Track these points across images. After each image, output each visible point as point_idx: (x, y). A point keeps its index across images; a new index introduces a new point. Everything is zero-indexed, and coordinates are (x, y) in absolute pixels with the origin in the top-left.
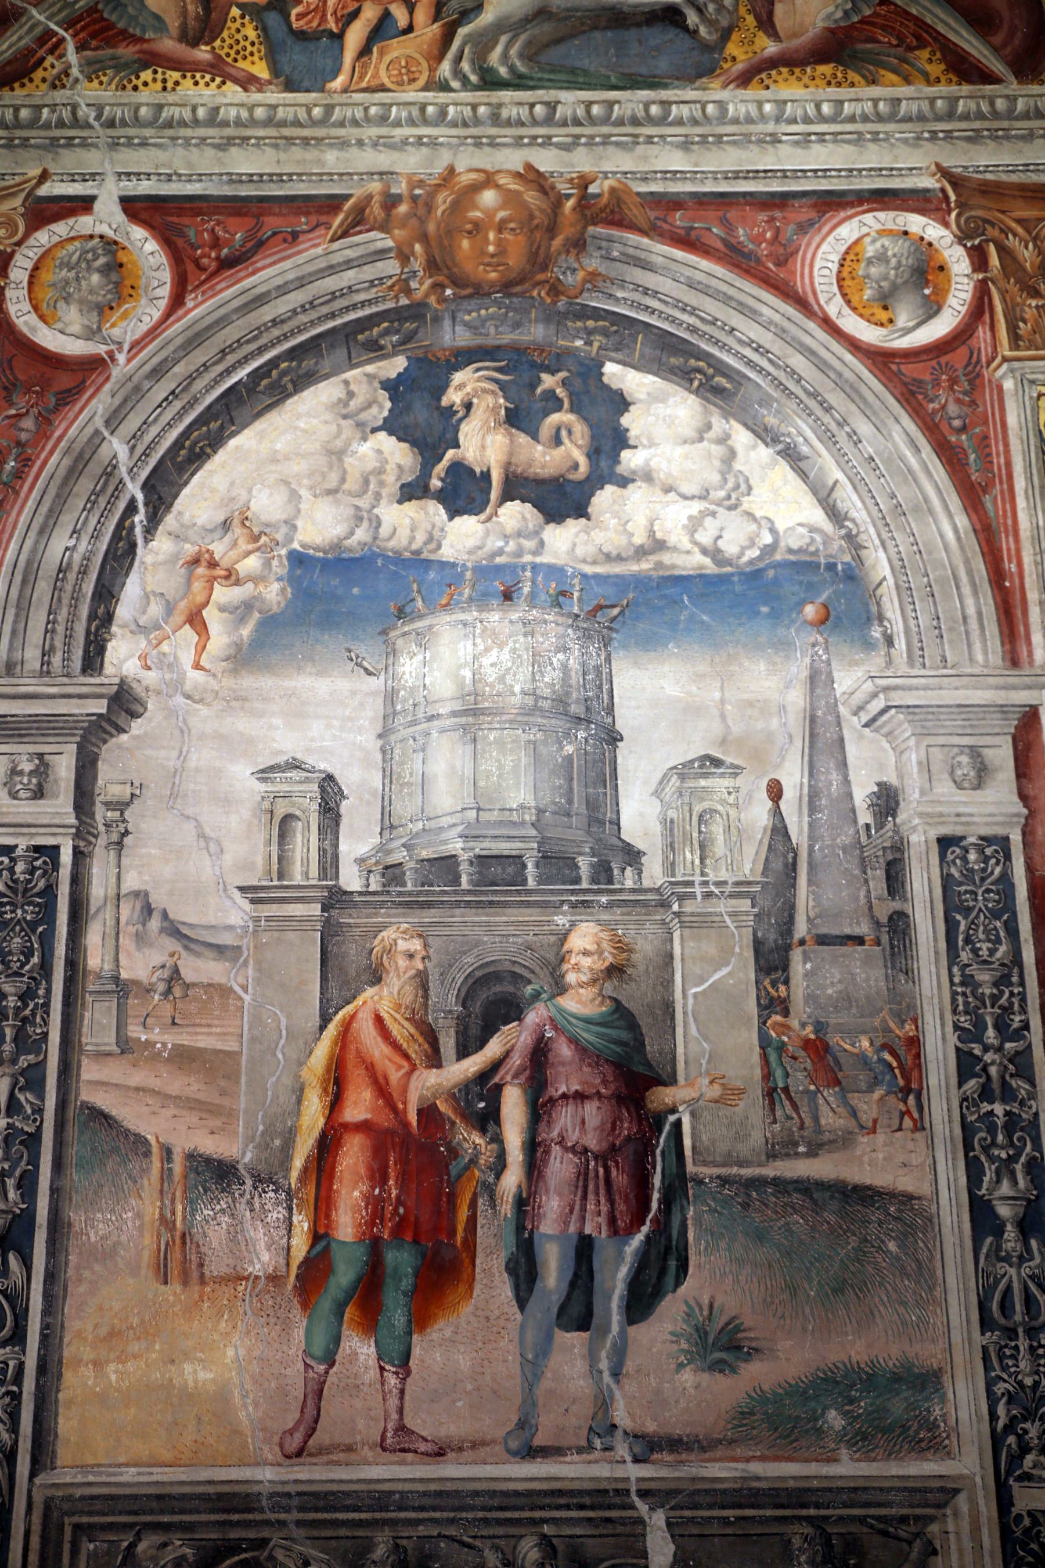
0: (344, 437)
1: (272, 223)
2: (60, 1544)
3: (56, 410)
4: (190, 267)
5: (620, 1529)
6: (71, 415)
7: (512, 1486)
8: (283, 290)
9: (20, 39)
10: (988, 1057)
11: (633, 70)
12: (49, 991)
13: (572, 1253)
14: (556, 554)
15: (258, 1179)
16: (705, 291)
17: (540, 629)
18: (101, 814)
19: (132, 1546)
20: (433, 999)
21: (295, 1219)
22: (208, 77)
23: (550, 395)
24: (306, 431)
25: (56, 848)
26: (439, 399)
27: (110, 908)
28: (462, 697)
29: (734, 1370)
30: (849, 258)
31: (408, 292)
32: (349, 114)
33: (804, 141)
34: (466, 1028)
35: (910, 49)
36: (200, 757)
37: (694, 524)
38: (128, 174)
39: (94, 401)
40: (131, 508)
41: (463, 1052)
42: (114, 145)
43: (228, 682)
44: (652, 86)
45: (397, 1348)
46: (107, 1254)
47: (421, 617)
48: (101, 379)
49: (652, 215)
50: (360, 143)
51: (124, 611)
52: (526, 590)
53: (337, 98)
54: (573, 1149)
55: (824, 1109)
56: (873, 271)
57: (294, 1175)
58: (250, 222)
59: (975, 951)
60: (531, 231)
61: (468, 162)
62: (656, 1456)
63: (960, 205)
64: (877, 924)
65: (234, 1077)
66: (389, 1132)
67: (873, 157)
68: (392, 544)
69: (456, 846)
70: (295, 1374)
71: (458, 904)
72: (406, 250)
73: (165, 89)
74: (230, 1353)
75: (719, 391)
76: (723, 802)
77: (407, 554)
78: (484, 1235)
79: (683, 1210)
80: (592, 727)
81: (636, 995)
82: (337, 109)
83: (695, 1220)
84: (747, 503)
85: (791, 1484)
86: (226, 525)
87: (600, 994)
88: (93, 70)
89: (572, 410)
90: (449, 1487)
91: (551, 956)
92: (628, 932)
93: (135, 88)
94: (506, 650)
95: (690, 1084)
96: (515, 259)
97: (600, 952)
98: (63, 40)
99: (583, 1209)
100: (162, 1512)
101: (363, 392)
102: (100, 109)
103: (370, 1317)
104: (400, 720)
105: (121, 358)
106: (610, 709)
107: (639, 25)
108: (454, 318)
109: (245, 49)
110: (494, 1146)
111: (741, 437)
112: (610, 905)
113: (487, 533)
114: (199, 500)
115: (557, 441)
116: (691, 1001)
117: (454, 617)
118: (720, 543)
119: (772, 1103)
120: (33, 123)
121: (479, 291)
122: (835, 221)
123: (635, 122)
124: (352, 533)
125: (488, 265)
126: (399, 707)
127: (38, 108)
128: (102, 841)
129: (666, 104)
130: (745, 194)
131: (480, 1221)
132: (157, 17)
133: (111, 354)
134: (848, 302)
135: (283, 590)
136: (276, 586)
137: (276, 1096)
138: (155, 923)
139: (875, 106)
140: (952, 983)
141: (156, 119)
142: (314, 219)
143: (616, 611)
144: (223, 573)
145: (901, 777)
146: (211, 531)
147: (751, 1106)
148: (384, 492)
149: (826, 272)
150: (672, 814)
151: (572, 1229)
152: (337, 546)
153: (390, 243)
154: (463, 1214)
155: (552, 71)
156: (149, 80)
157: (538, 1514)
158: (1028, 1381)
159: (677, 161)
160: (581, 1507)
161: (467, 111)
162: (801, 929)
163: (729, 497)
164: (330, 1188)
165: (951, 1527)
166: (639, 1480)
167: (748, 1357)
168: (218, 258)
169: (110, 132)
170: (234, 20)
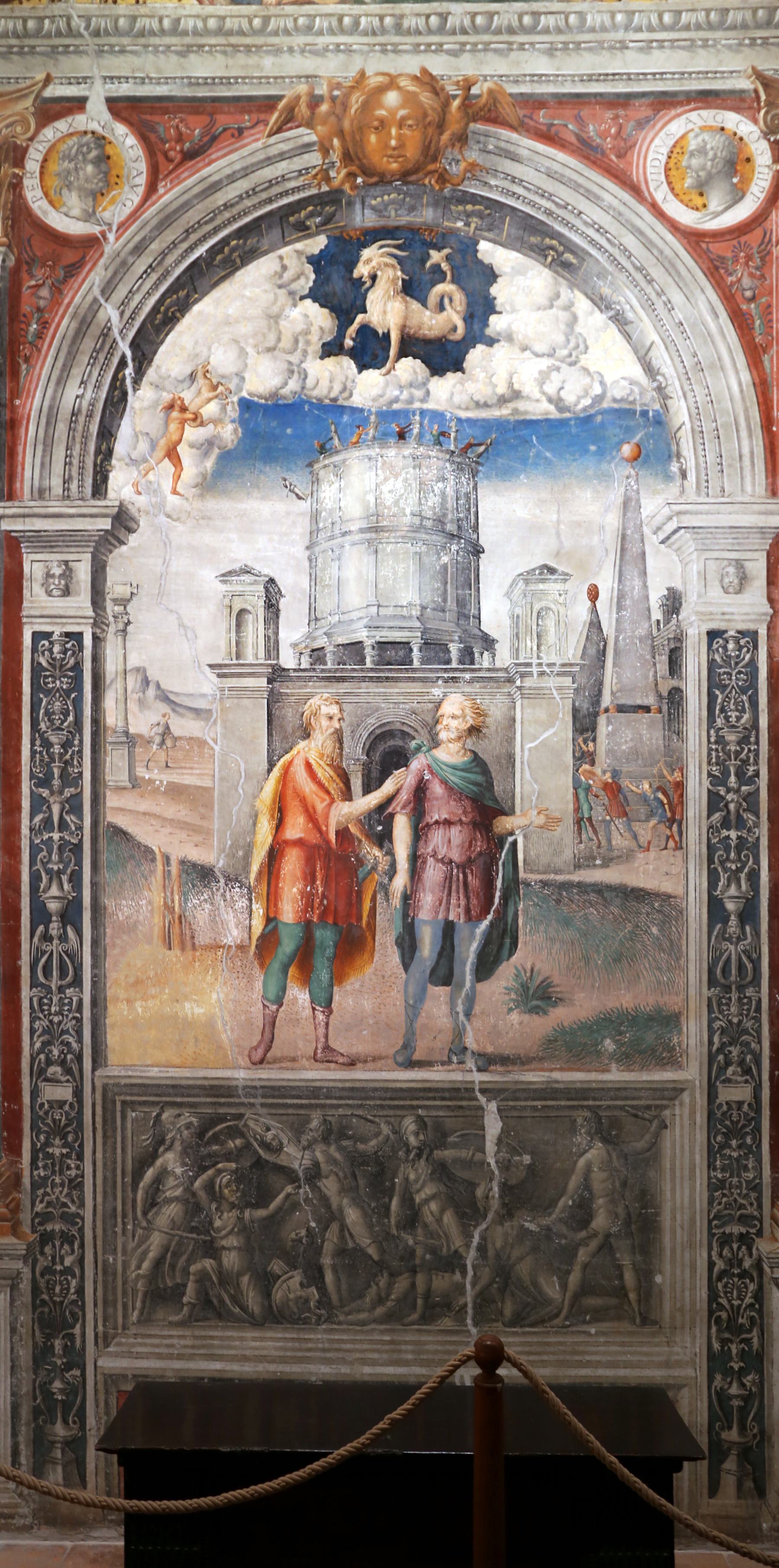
0: (279, 304)
1: (222, 120)
2: (114, 1112)
3: (65, 281)
4: (161, 159)
5: (468, 1113)
6: (76, 285)
7: (398, 1085)
8: (232, 178)
10: (729, 797)
12: (81, 741)
13: (440, 933)
14: (438, 402)
15: (228, 879)
17: (426, 462)
18: (111, 609)
19: (159, 1115)
20: (346, 750)
21: (254, 907)
23: (437, 268)
24: (250, 299)
25: (80, 634)
26: (352, 272)
27: (120, 680)
28: (368, 517)
29: (545, 1013)
31: (328, 179)
32: (282, 24)
34: (369, 771)
36: (179, 563)
37: (543, 378)
38: (112, 78)
39: (92, 274)
40: (123, 364)
41: (367, 789)
42: (100, 52)
43: (197, 504)
45: (323, 996)
46: (130, 928)
47: (337, 452)
48: (97, 255)
50: (291, 50)
51: (121, 447)
52: (416, 431)
54: (442, 861)
55: (615, 834)
57: (253, 876)
58: (206, 119)
59: (727, 718)
61: (376, 66)
62: (492, 1068)
64: (660, 696)
65: (209, 806)
66: (317, 847)
68: (315, 393)
69: (362, 635)
70: (257, 1010)
71: (363, 679)
72: (327, 144)
74: (214, 996)
75: (566, 265)
76: (556, 602)
77: (327, 401)
78: (381, 920)
79: (516, 904)
80: (461, 539)
81: (488, 749)
82: (273, 20)
83: (524, 911)
84: (584, 360)
85: (579, 1085)
86: (192, 377)
87: (464, 748)
89: (453, 281)
90: (358, 1085)
91: (429, 719)
92: (484, 702)
94: (400, 479)
95: (524, 814)
96: (412, 152)
97: (464, 716)
99: (448, 903)
100: (176, 1095)
101: (294, 265)
103: (306, 976)
104: (322, 535)
105: (111, 237)
106: (476, 528)
108: (363, 203)
110: (388, 858)
111: (582, 304)
112: (472, 681)
113: (387, 384)
114: (173, 355)
115: (441, 308)
116: (526, 753)
117: (362, 453)
118: (562, 393)
119: (580, 829)
121: (382, 180)
124: (286, 384)
126: (321, 525)
128: (112, 629)
131: (379, 910)
133: (103, 234)
135: (235, 430)
136: (230, 427)
137: (238, 820)
138: (151, 692)
140: (709, 742)
141: (132, 28)
142: (255, 116)
143: (482, 448)
144: (191, 416)
145: (685, 583)
146: (182, 382)
147: (565, 831)
148: (310, 349)
150: (518, 611)
151: (441, 916)
152: (275, 395)
153: (314, 138)
154: (367, 905)
157: (415, 1103)
158: (735, 1020)
160: (443, 1099)
161: (376, 22)
162: (606, 700)
163: (570, 355)
164: (277, 886)
165: (677, 1112)
166: (481, 1082)
167: (555, 1004)
168: (182, 151)
169: (98, 41)
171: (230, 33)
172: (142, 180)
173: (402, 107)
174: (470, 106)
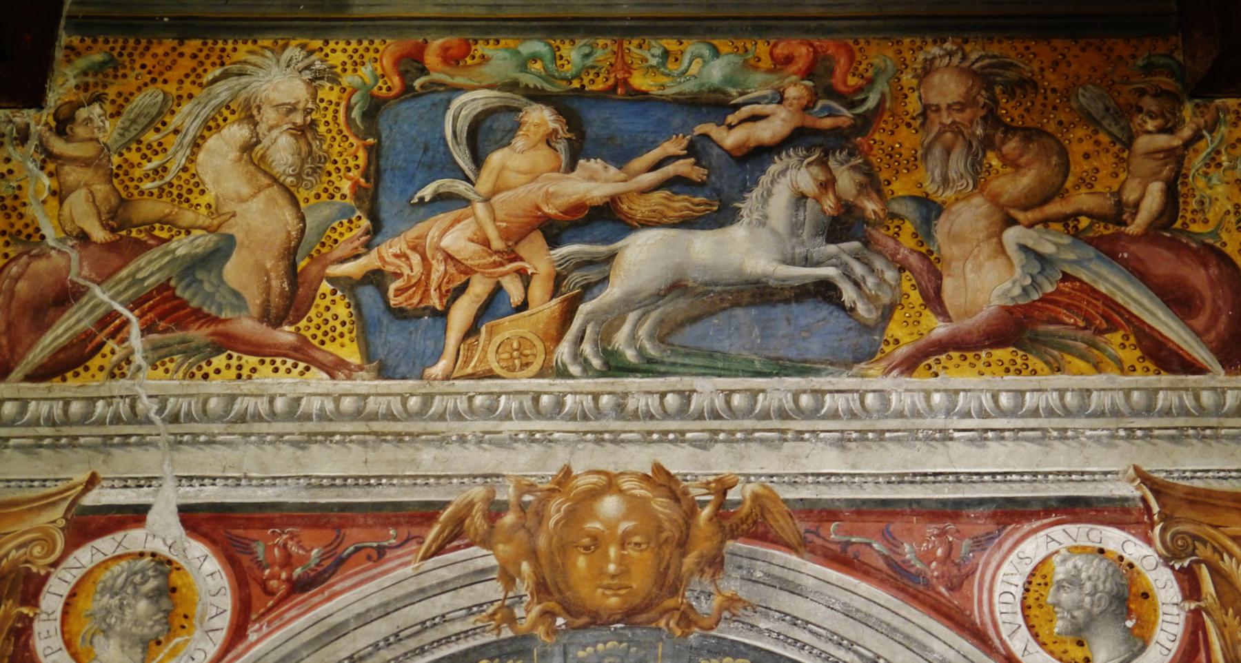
1: (355, 536)
4: (256, 591)
8: (364, 619)
9: (79, 321)
11: (781, 354)
16: (865, 621)
22: (290, 362)
30: (1036, 580)
31: (512, 620)
32: (451, 405)
33: (980, 438)
35: (1100, 332)
38: (190, 478)
42: (177, 443)
44: (803, 372)
49: (802, 526)
50: (462, 439)
53: (439, 386)
56: (1065, 597)
58: (330, 535)
60: (660, 546)
61: (586, 462)
63: (1165, 517)
67: (1060, 458)
72: (511, 570)
73: (239, 377)
82: (437, 398)
88: (158, 356)
93: (206, 376)
96: (640, 582)
98: (127, 322)
102: (163, 400)
107: (787, 301)
108: (565, 654)
109: (334, 329)
120: (85, 419)
121: (596, 620)
122: (1017, 535)
123: (783, 415)
125: (608, 587)
127: (92, 400)
129: (818, 393)
130: (910, 502)
132: (236, 294)
134: (1036, 636)
139: (1062, 398)
141: (227, 412)
142: (404, 531)
149: (1008, 598)
153: (492, 561)
155: (687, 355)
156: (222, 367)
159: (830, 461)
161: (588, 401)
168: (289, 580)
169: (174, 428)
170: (324, 296)
171: (374, 417)
172: (223, 622)
173: (626, 517)
174: (726, 516)
